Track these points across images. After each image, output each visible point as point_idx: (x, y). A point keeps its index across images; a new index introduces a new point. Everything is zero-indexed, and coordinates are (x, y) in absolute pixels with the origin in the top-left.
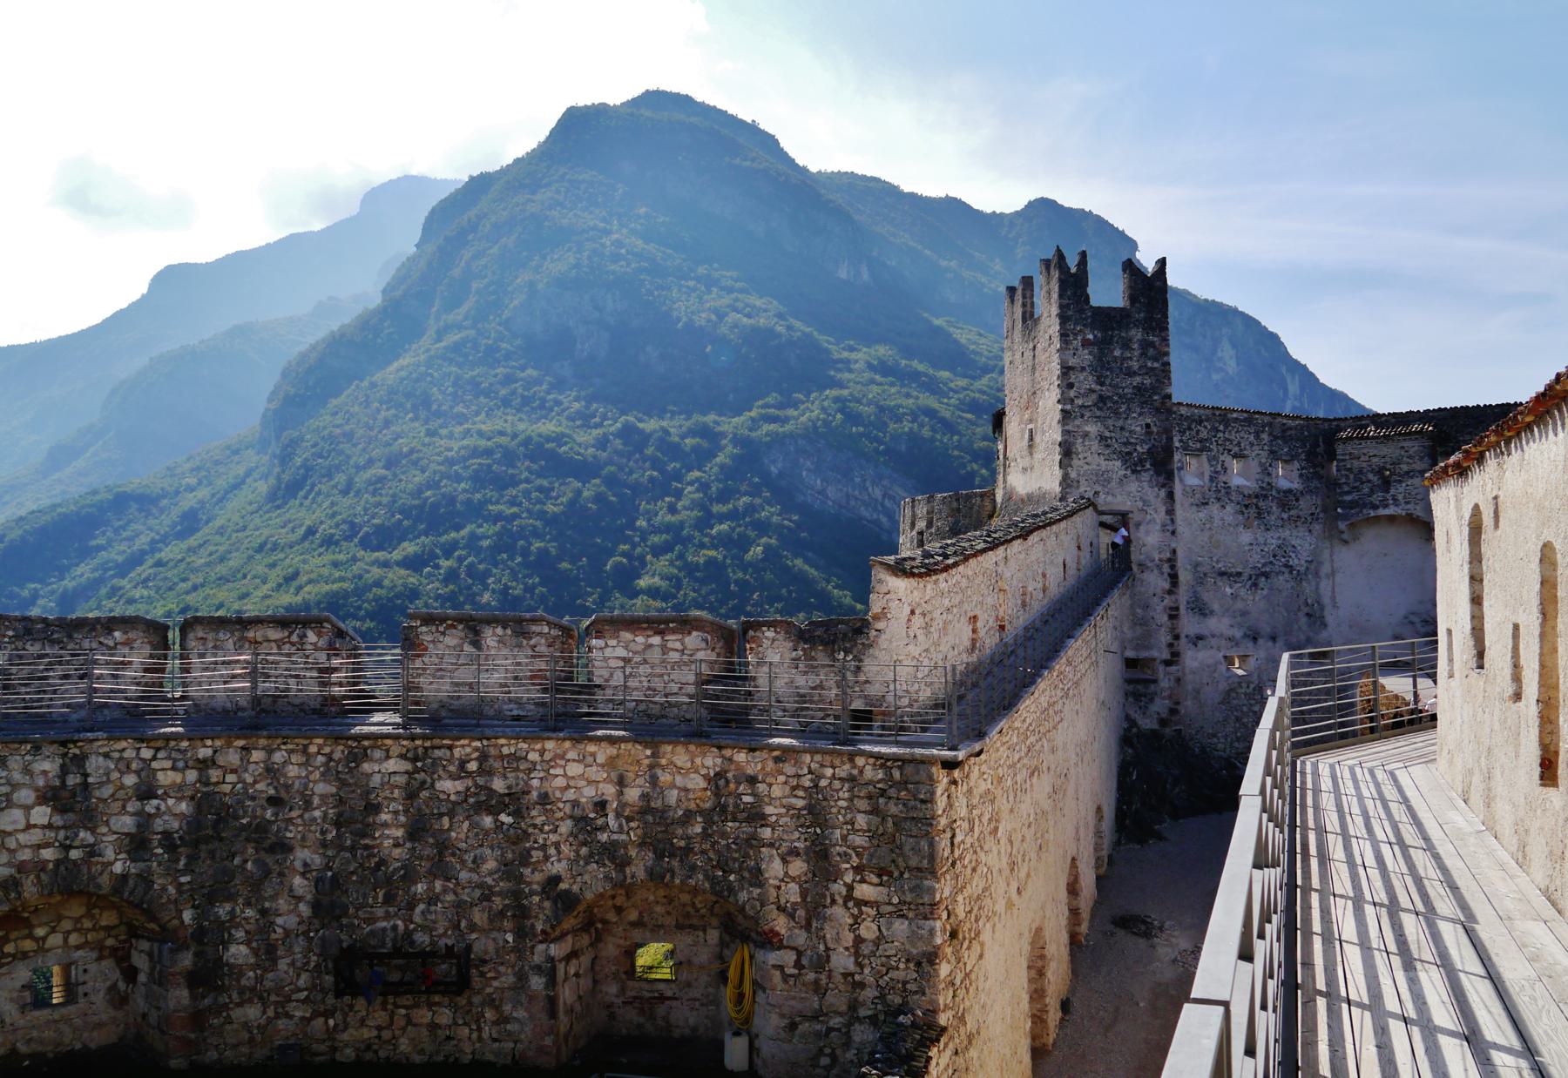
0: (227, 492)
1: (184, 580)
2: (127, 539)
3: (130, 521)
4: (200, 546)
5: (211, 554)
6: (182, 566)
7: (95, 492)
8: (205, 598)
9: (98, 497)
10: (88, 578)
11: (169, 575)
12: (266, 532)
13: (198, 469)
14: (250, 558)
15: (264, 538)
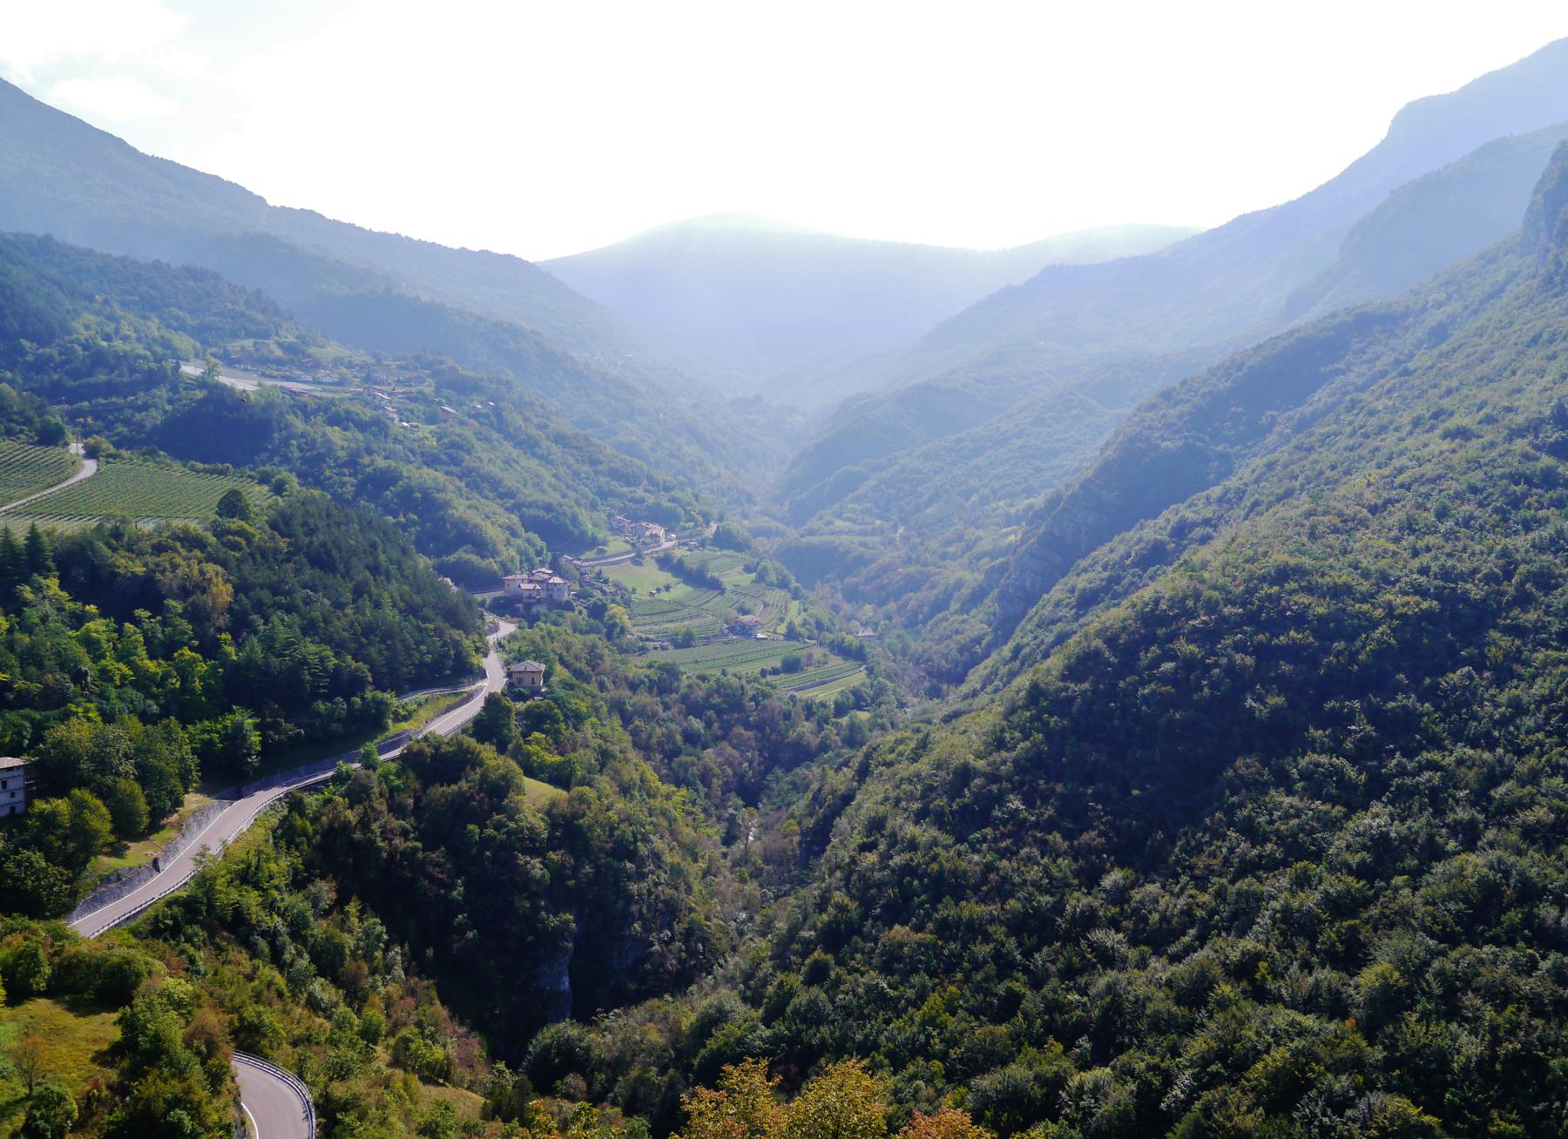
0: (1482, 303)
1: (1435, 386)
2: (1366, 362)
3: (1371, 343)
4: (1454, 350)
5: (1468, 356)
6: (1434, 371)
7: (1334, 315)
8: (1461, 401)
9: (1337, 321)
10: (1326, 403)
11: (1417, 382)
12: (1540, 324)
13: (1447, 283)
14: (1520, 353)
15: (1537, 330)
